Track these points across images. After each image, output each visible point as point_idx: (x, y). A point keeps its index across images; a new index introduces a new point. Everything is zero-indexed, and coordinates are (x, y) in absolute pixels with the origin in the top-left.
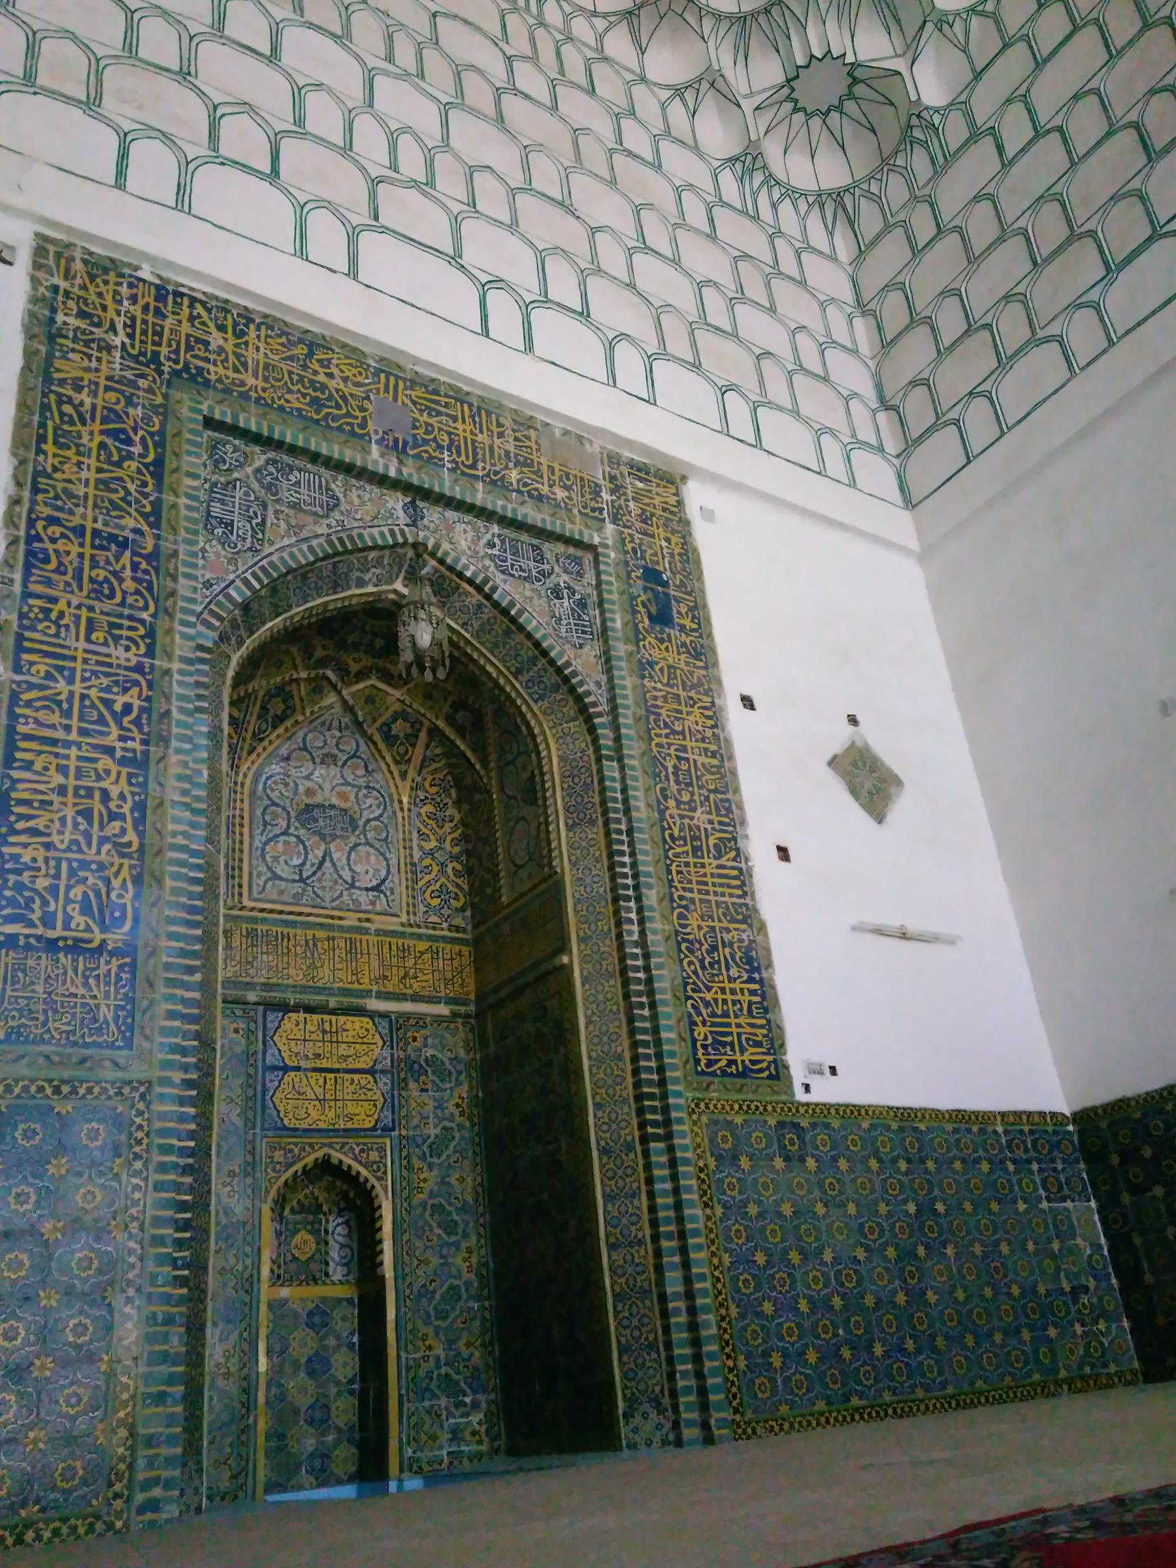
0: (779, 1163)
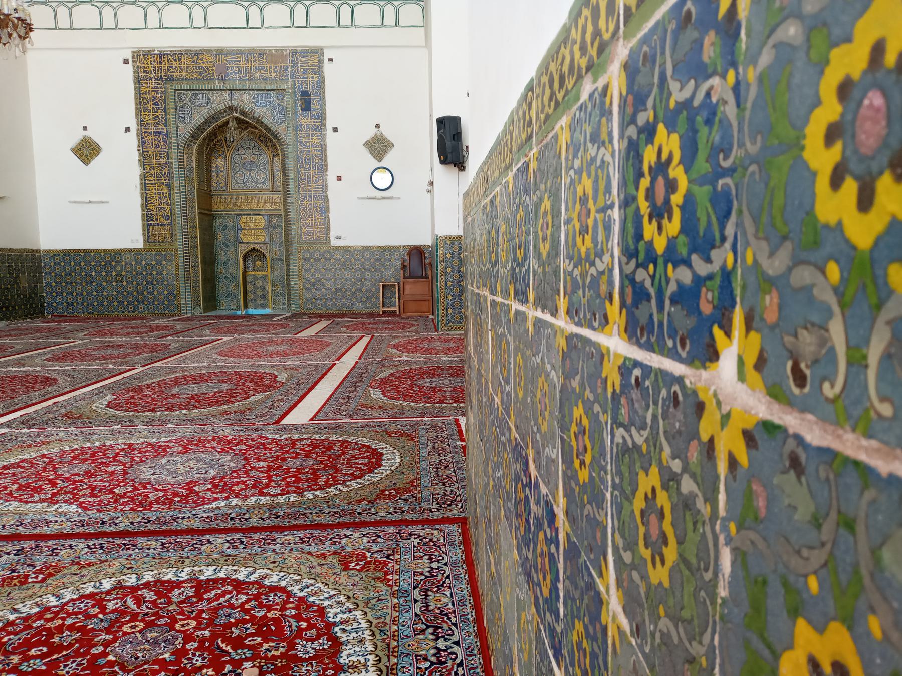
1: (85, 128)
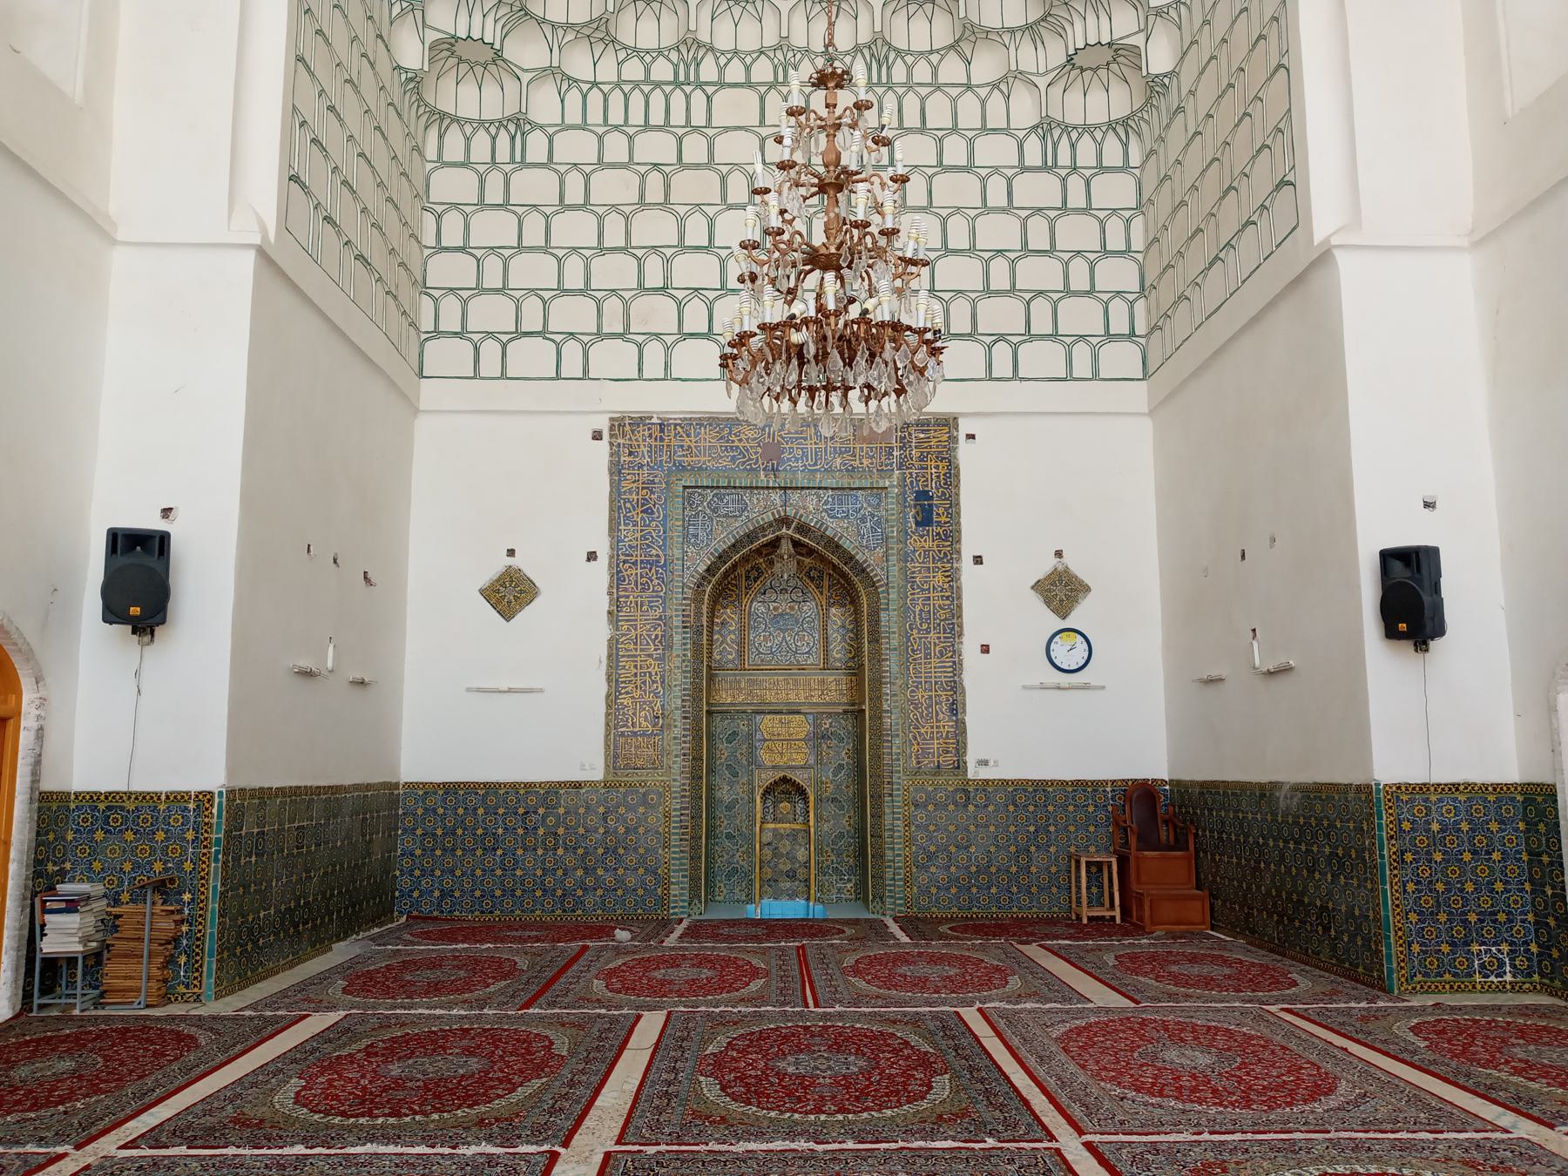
0: (951, 807)
1: (511, 553)
